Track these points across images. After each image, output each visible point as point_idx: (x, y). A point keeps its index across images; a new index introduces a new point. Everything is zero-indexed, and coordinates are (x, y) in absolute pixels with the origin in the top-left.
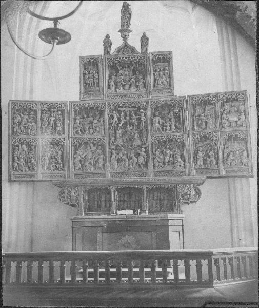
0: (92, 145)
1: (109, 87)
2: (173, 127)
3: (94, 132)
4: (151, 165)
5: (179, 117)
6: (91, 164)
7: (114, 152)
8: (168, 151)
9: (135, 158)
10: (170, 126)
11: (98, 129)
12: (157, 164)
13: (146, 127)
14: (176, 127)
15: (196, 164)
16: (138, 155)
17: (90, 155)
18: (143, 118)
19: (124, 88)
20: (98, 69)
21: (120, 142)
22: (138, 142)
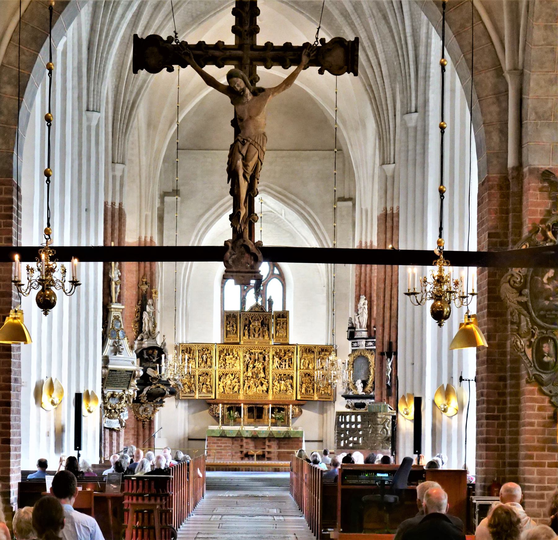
0: (231, 376)
1: (244, 335)
2: (287, 366)
3: (233, 367)
4: (270, 392)
5: (291, 359)
6: (230, 388)
7: (246, 381)
8: (283, 382)
9: (260, 386)
10: (285, 365)
11: (235, 365)
12: (275, 390)
13: (268, 364)
14: (289, 366)
15: (301, 392)
16: (262, 384)
17: (229, 382)
18: (267, 359)
19: (254, 336)
20: (236, 320)
21: (250, 374)
22: (262, 375)
